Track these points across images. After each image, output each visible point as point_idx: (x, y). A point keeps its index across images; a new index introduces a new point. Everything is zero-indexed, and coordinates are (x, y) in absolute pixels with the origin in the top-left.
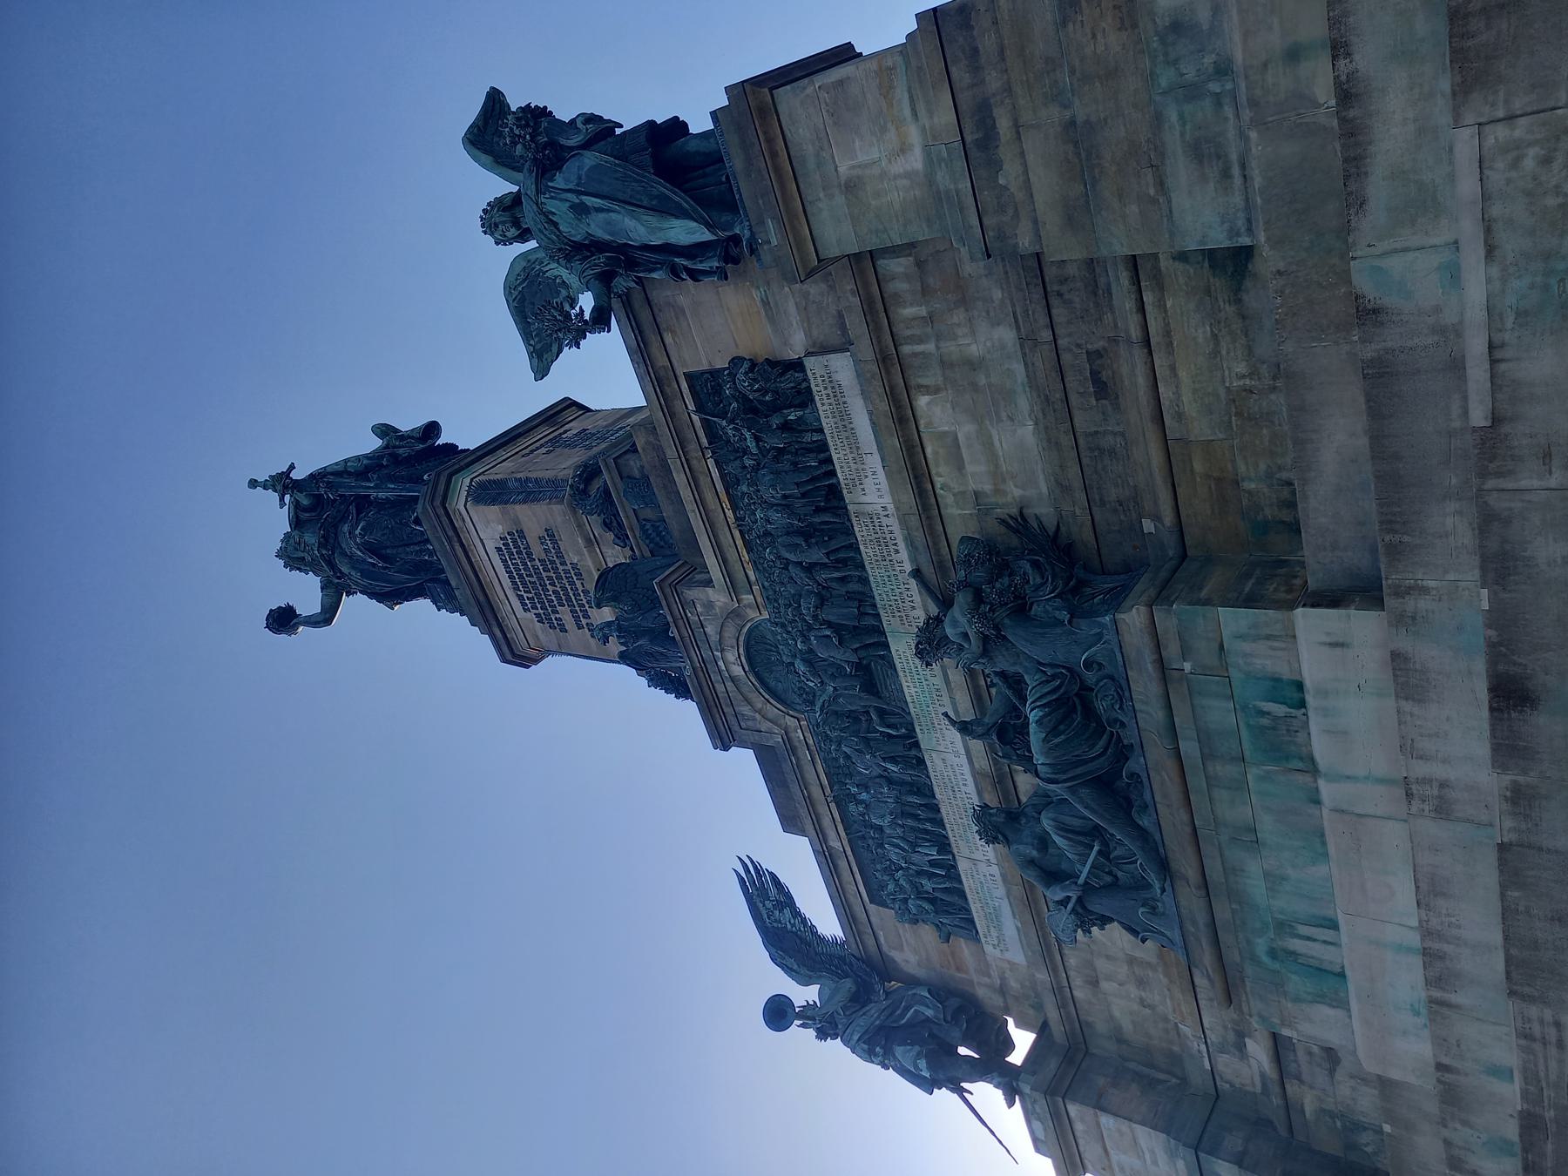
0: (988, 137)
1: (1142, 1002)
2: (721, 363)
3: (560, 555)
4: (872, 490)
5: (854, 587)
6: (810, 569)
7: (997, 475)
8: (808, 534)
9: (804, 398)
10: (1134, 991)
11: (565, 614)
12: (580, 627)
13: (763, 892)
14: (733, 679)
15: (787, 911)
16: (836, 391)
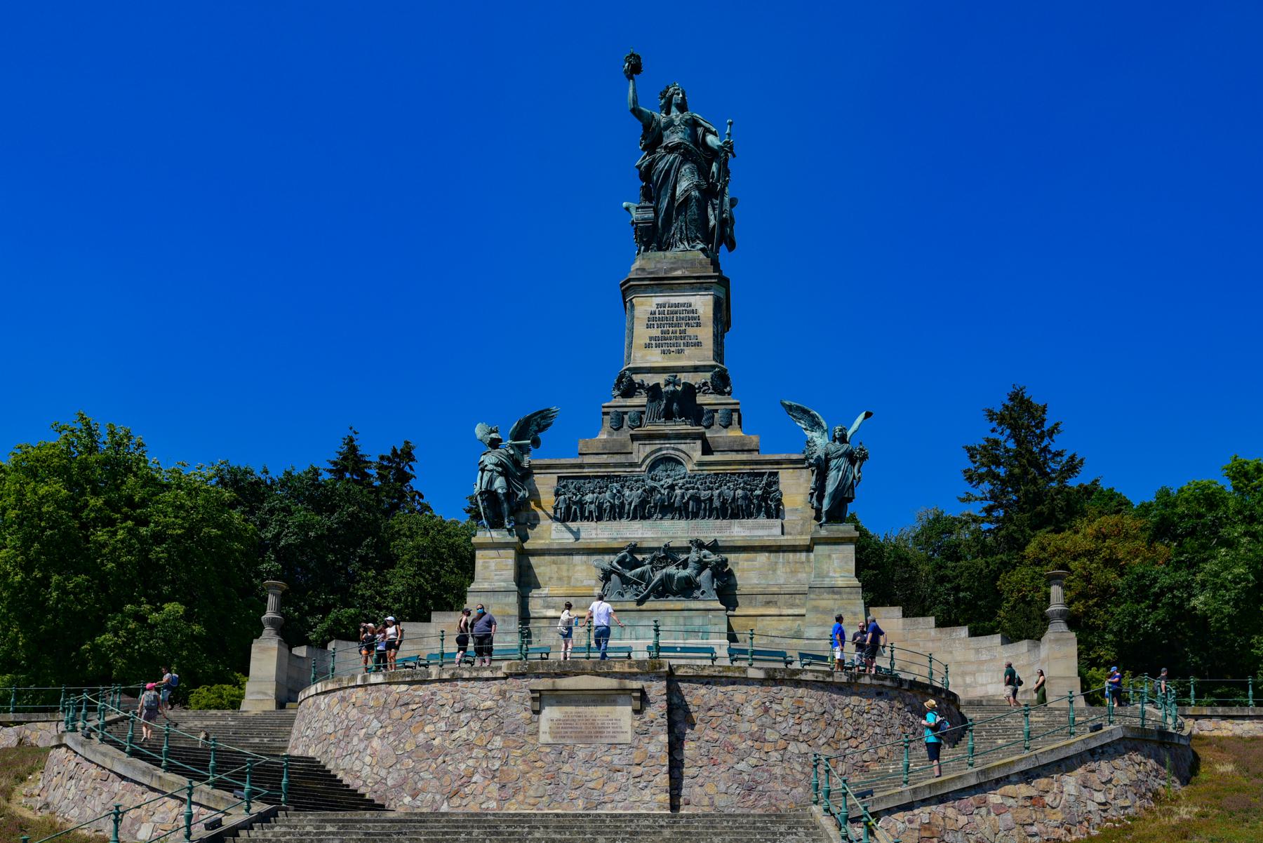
0: (834, 593)
1: (550, 578)
2: (781, 487)
3: (687, 345)
4: (737, 531)
5: (702, 513)
6: (711, 499)
7: (743, 571)
8: (724, 503)
9: (769, 516)
10: (555, 576)
11: (656, 332)
12: (651, 338)
13: (544, 418)
14: (660, 449)
15: (536, 428)
16: (770, 527)
